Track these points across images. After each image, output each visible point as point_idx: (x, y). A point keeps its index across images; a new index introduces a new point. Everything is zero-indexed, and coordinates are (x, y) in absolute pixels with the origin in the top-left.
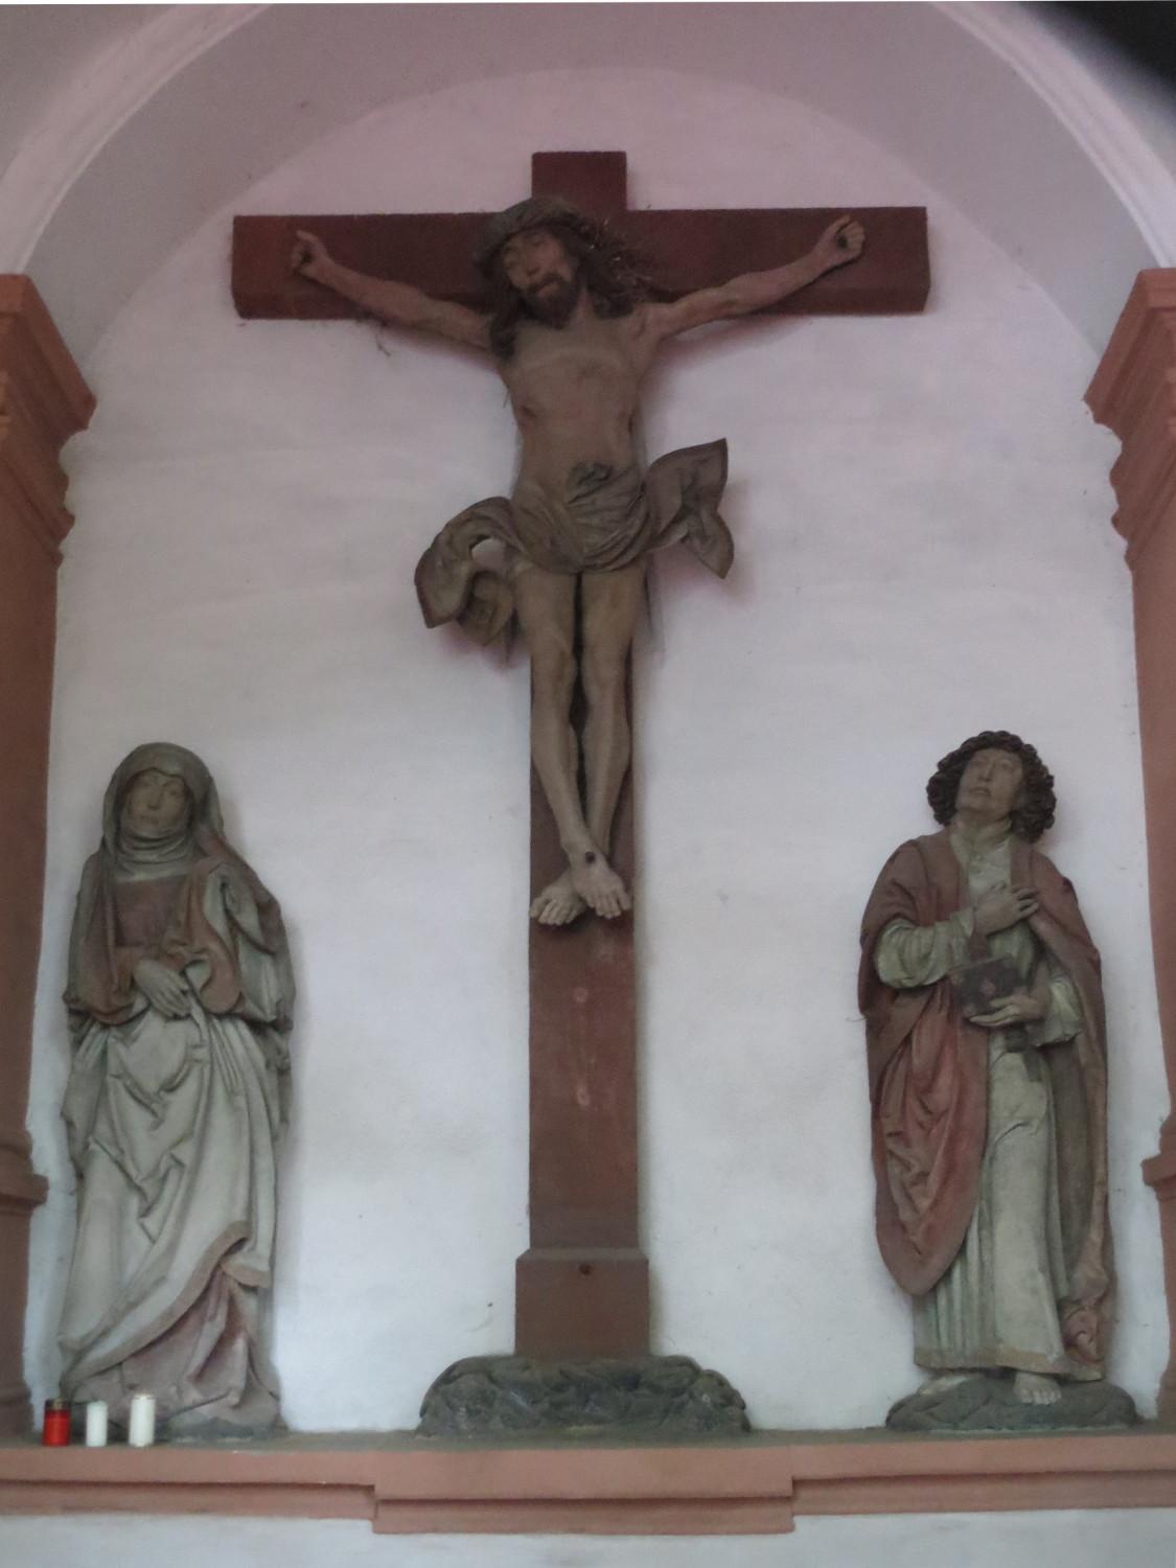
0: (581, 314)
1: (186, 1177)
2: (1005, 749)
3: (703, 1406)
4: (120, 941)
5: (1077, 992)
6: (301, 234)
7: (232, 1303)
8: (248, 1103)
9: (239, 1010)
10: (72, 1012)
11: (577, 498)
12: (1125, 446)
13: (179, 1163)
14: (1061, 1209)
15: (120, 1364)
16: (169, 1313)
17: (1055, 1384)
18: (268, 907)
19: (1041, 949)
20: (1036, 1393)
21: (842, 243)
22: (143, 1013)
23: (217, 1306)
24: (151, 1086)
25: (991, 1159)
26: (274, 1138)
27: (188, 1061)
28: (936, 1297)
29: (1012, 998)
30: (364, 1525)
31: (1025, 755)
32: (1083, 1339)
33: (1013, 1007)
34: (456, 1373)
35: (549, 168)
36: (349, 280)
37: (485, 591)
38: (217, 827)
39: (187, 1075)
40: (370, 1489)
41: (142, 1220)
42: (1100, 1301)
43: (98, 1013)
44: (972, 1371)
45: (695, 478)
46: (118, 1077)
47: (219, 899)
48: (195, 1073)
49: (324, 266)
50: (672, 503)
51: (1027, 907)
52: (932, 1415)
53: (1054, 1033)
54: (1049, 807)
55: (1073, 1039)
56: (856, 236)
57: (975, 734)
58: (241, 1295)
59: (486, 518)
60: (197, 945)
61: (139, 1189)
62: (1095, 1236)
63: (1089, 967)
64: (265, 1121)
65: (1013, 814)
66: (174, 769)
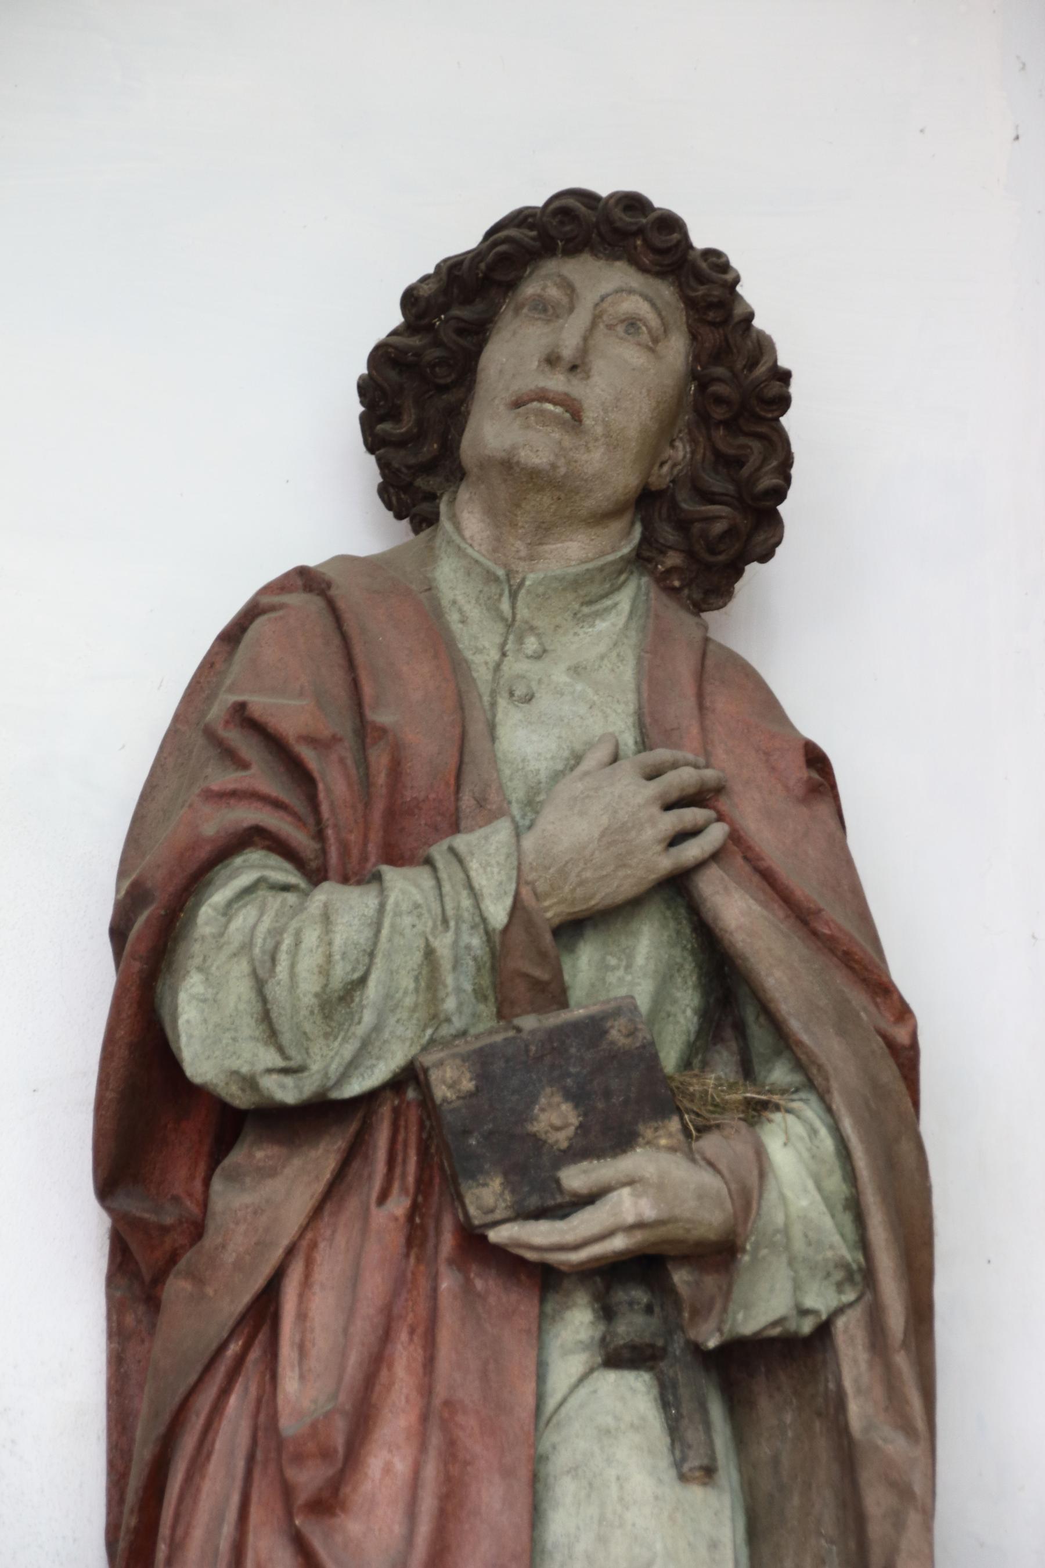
19: (724, 980)
33: (640, 1191)
53: (765, 1301)
65: (646, 502)
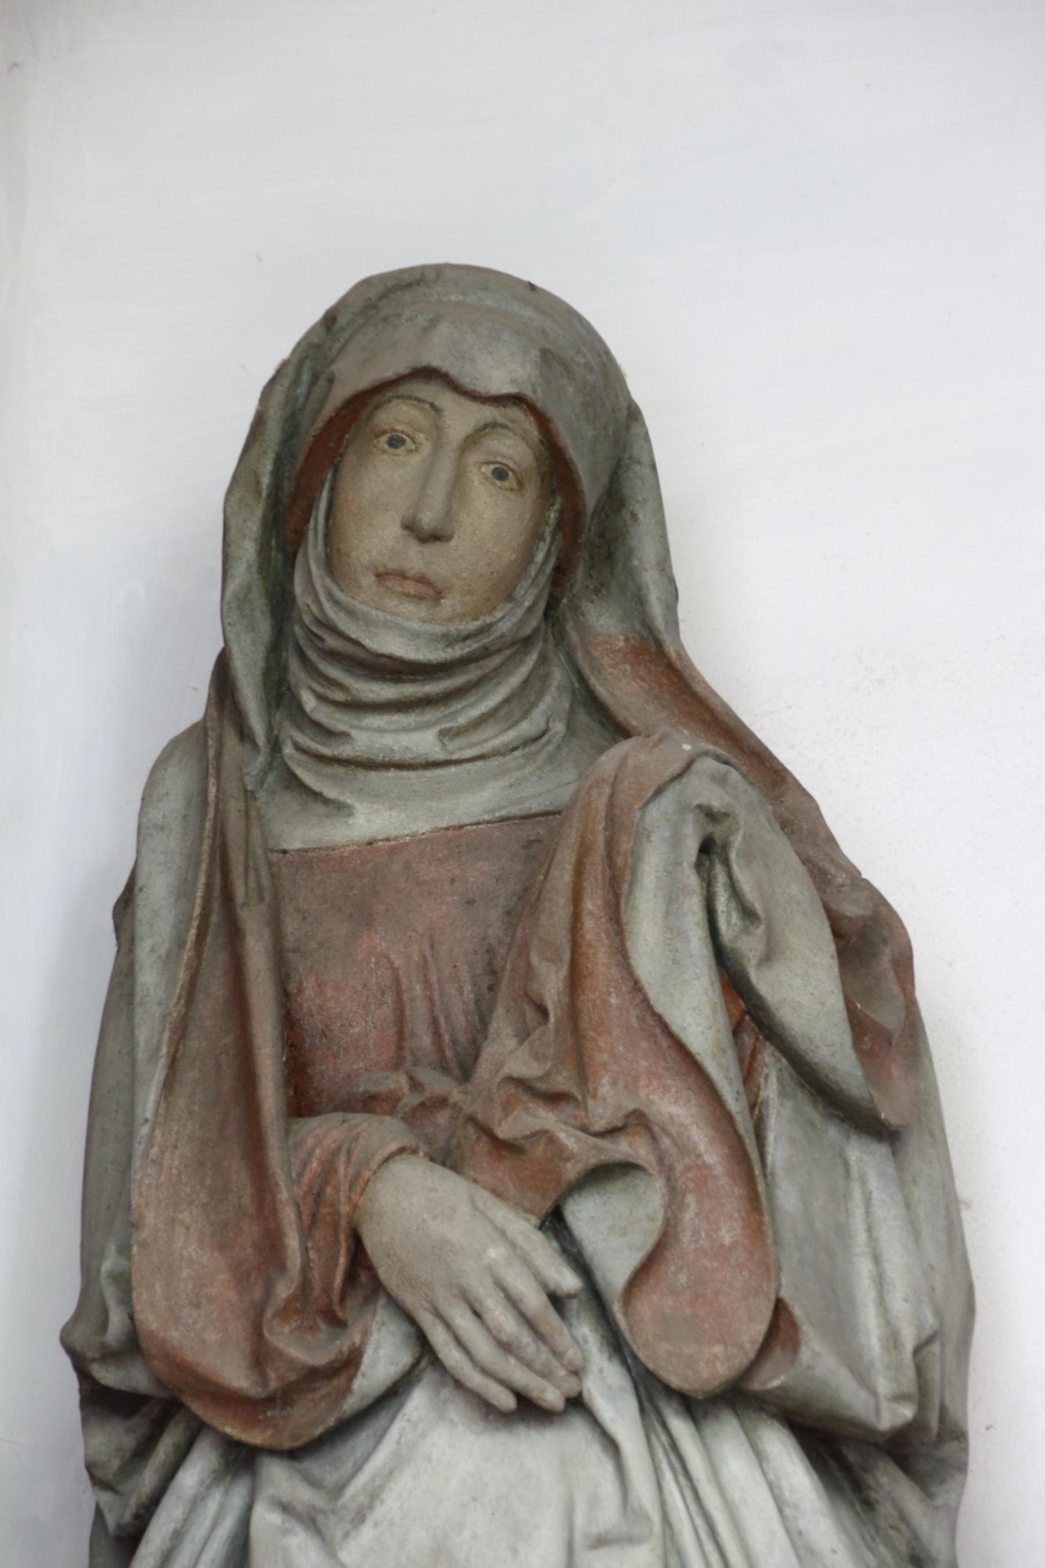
9: (772, 1379)
47: (694, 905)
60: (608, 1101)
66: (502, 370)
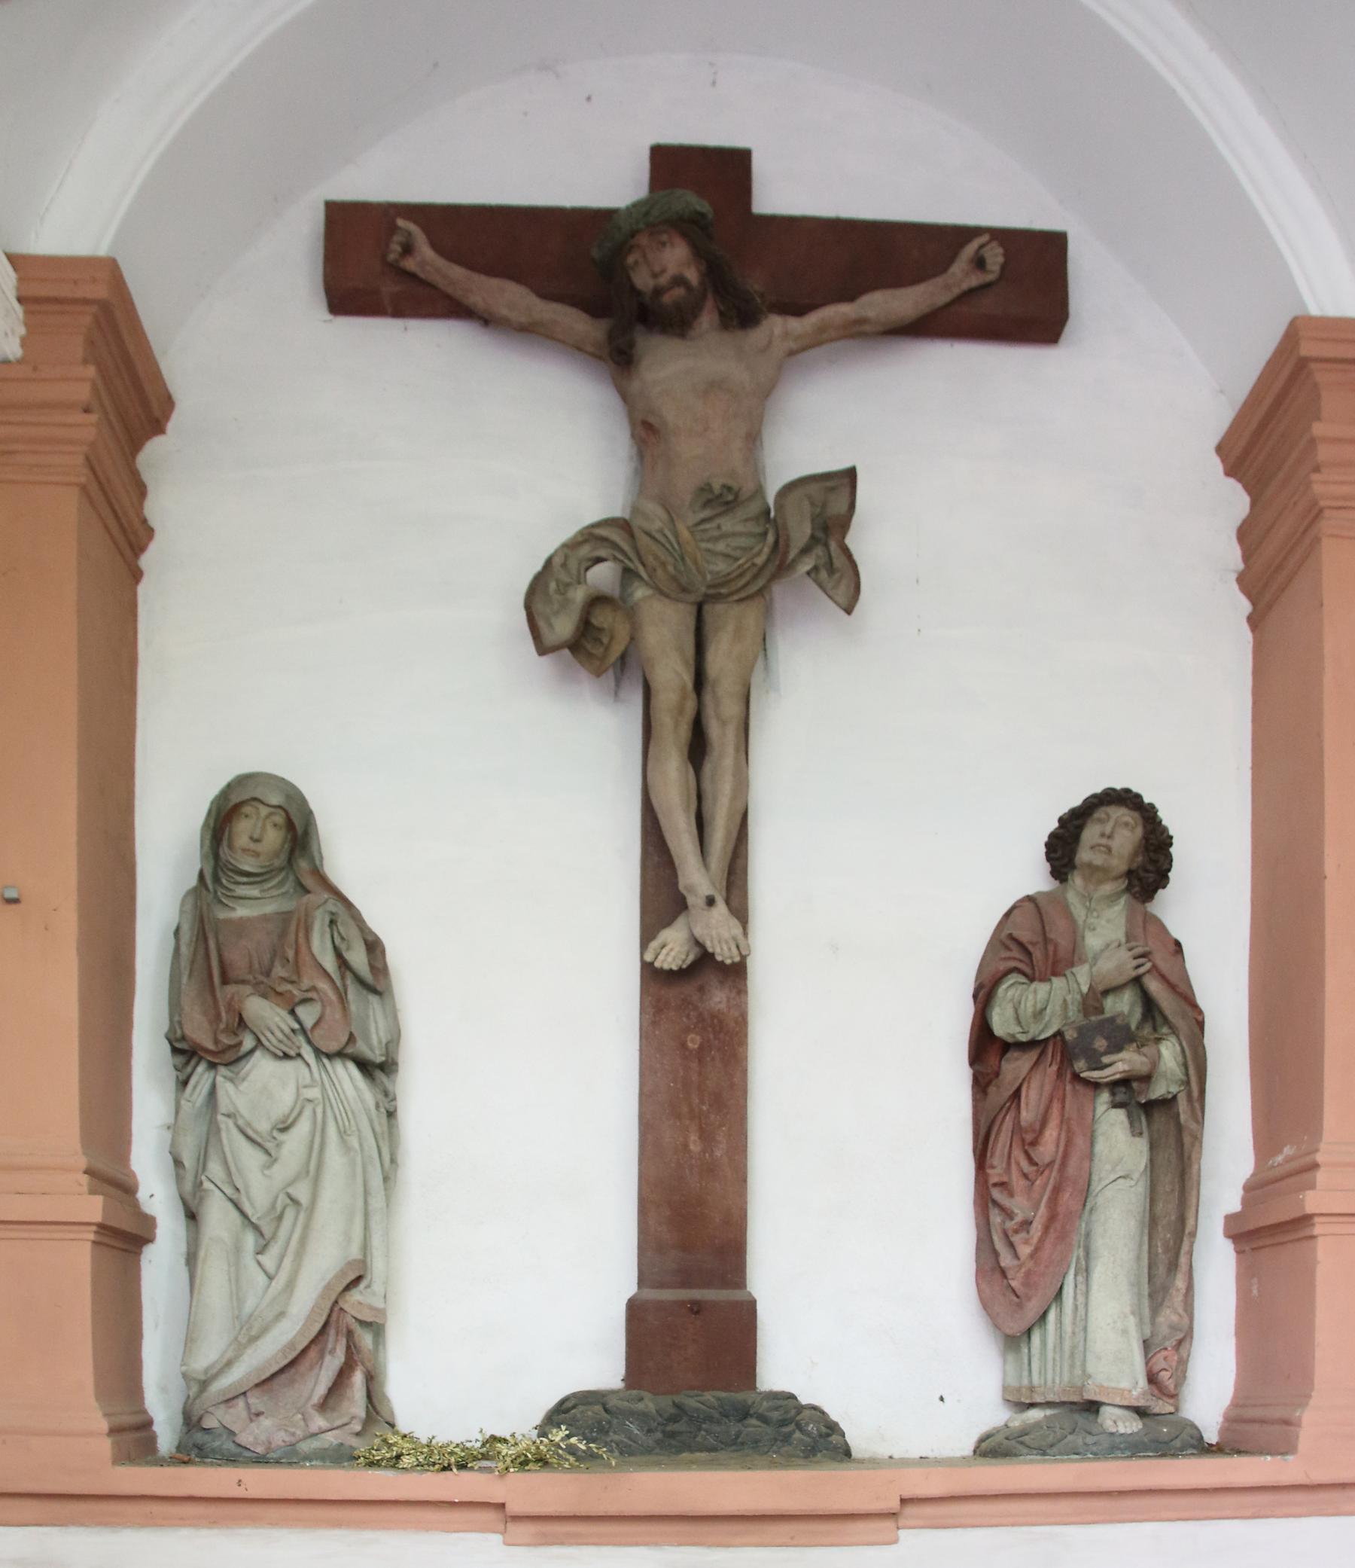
0: (707, 319)
1: (302, 1216)
2: (1127, 806)
3: (806, 1435)
4: (225, 981)
5: (1183, 1051)
6: (401, 222)
7: (350, 1334)
8: (361, 1145)
9: (349, 1050)
10: (175, 1051)
11: (703, 521)
12: (1253, 505)
13: (295, 1202)
14: (1150, 1258)
15: (244, 1393)
16: (291, 1345)
17: (1136, 1416)
18: (374, 947)
19: (1149, 1005)
20: (1118, 1422)
21: (980, 263)
22: (251, 1052)
23: (337, 1341)
24: (263, 1126)
25: (1092, 1210)
26: (386, 1179)
27: (302, 1104)
28: (1029, 1337)
29: (1121, 1055)
30: (496, 1539)
31: (1148, 814)
32: (1164, 1376)
33: (1123, 1063)
34: (569, 1404)
35: (670, 163)
36: (453, 275)
37: (602, 618)
38: (318, 863)
39: (300, 1114)
40: (502, 1506)
41: (260, 1257)
42: (1180, 1342)
43: (204, 1050)
44: (1063, 1404)
45: (824, 505)
46: (228, 1116)
47: (328, 936)
48: (307, 1113)
49: (426, 259)
50: (800, 531)
51: (1138, 967)
52: (1022, 1443)
53: (1159, 1090)
54: (1165, 867)
55: (1175, 1097)
56: (995, 257)
57: (1098, 790)
58: (358, 1330)
59: (604, 540)
60: (306, 983)
61: (256, 1228)
62: (1180, 1283)
63: (1194, 1024)
64: (378, 1165)
65: (1130, 874)
66: (275, 800)
